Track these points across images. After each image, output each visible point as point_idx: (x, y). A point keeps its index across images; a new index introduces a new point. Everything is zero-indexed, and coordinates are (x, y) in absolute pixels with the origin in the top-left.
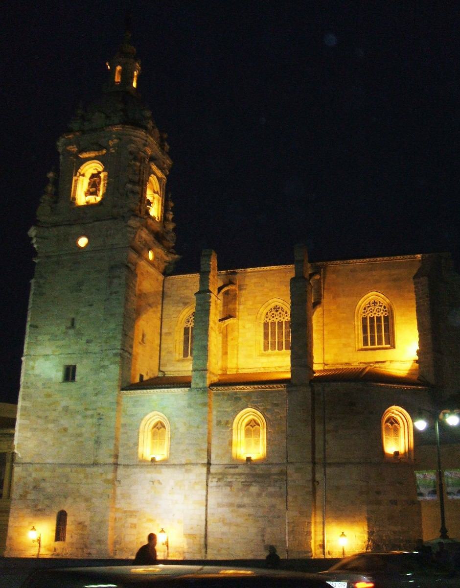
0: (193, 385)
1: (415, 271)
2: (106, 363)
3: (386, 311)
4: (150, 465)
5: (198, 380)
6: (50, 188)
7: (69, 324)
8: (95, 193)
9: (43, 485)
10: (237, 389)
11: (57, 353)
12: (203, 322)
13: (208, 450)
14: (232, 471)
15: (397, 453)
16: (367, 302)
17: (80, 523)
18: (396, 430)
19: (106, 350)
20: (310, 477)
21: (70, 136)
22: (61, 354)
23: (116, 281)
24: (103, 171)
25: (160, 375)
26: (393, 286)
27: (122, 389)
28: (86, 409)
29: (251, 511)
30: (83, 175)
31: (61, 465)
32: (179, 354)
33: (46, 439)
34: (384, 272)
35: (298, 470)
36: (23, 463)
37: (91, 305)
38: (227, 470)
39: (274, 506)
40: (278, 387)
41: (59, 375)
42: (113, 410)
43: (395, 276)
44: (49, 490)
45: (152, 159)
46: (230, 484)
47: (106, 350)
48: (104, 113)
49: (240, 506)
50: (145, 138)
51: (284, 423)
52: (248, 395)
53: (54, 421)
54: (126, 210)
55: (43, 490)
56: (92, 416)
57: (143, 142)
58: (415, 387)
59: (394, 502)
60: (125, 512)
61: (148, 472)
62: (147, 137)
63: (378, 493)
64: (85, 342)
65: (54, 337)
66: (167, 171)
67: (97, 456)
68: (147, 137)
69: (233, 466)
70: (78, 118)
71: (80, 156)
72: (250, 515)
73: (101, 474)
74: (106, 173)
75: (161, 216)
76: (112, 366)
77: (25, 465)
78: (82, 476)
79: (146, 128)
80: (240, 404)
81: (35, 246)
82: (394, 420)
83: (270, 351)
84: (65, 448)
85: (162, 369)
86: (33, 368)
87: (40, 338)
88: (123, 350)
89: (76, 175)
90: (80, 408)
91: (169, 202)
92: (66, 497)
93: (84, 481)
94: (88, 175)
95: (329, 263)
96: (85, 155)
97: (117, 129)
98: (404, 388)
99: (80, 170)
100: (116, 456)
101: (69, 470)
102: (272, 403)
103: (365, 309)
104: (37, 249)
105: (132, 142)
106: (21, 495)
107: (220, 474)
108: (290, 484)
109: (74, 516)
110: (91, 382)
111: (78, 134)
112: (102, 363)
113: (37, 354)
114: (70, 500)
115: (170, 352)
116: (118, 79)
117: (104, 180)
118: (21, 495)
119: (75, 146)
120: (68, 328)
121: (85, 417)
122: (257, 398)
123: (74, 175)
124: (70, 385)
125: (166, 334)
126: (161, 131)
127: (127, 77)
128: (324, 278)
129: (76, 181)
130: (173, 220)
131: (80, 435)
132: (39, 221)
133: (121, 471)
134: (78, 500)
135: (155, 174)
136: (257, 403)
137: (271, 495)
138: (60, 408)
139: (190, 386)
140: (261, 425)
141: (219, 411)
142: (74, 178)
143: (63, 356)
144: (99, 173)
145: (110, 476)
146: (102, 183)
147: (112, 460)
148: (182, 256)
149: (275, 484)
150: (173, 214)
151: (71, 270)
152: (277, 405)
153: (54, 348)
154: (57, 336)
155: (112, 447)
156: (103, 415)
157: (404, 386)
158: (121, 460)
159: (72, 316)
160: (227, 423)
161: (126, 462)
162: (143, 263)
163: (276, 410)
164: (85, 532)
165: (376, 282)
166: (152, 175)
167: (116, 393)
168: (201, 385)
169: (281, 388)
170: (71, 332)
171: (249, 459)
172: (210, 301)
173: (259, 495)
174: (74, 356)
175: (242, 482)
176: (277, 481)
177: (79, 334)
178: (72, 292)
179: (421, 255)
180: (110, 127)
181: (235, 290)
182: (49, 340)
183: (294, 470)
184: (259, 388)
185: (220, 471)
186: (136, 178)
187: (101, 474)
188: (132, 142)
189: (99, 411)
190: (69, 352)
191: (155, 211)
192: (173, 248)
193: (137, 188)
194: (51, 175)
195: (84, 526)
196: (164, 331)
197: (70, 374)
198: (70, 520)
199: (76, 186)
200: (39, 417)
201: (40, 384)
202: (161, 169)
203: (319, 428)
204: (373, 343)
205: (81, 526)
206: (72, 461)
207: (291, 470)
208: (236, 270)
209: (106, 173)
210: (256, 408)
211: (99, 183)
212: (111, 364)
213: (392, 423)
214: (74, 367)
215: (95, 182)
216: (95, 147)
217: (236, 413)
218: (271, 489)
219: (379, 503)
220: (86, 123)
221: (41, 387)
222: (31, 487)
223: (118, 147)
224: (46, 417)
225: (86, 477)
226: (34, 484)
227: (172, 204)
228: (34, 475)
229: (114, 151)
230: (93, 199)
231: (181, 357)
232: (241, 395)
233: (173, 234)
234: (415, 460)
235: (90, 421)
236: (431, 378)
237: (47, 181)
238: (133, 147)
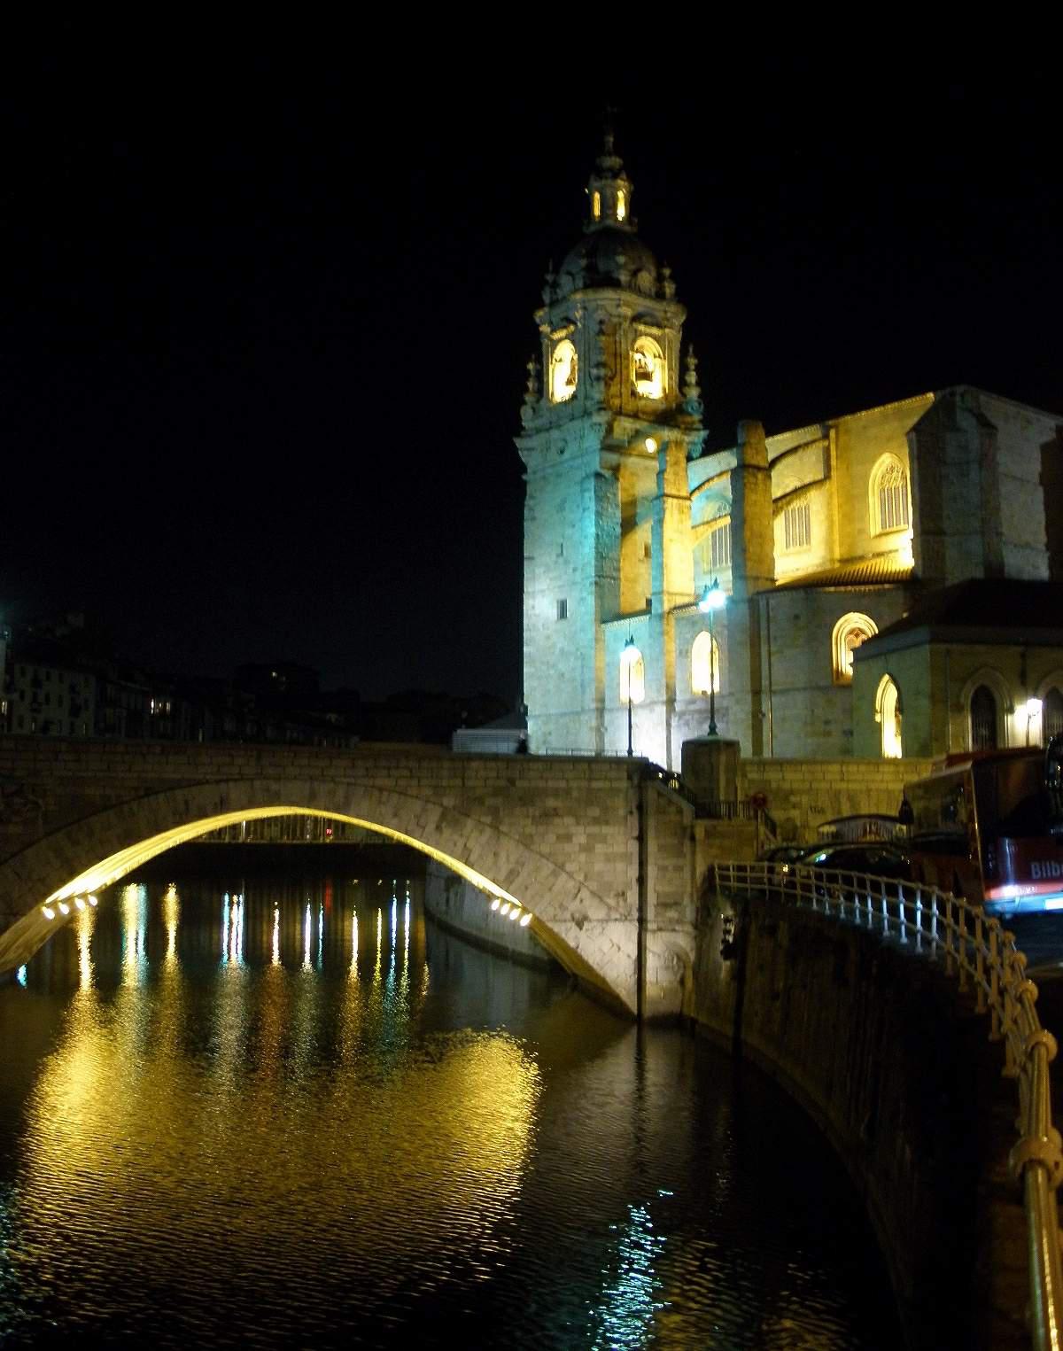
16: (883, 468)
27: (604, 622)
31: (564, 715)
35: (737, 702)
53: (554, 666)
57: (614, 303)
63: (827, 722)
80: (697, 629)
83: (792, 549)
86: (533, 607)
97: (579, 296)
120: (558, 556)
124: (563, 621)
127: (609, 205)
138: (557, 651)
147: (593, 706)
158: (608, 704)
159: (561, 540)
170: (561, 560)
177: (567, 562)
188: (597, 308)
200: (542, 663)
204: (720, 563)
217: (693, 638)
219: (828, 734)
237: (527, 374)
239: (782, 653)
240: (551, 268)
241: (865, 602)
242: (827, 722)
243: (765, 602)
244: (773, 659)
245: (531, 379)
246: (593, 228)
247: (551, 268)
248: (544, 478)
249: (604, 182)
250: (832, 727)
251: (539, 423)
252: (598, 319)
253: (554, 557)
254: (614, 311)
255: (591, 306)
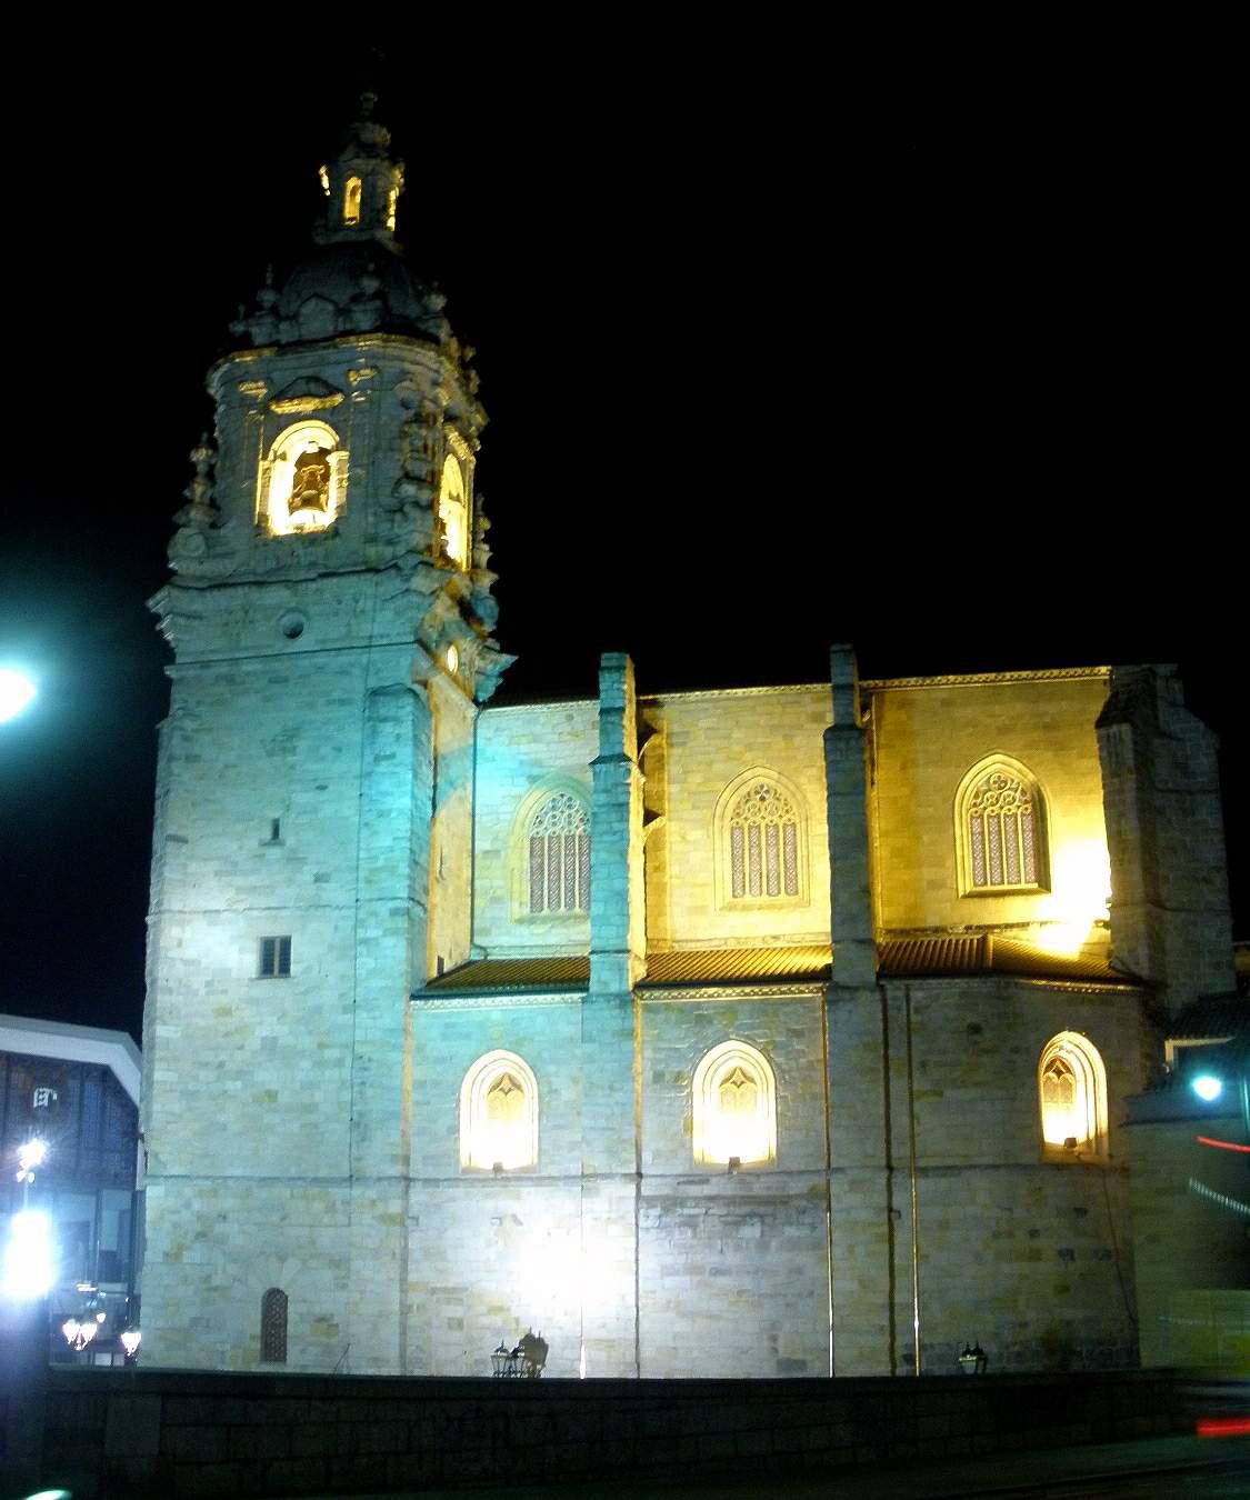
0: (594, 987)
1: (1096, 709)
2: (372, 933)
3: (1026, 802)
4: (493, 1180)
5: (606, 976)
6: (199, 489)
7: (267, 834)
8: (309, 502)
9: (220, 1228)
10: (701, 996)
11: (241, 906)
12: (615, 833)
13: (636, 1141)
14: (694, 1190)
15: (1071, 1142)
17: (321, 1319)
18: (1068, 1087)
19: (370, 900)
20: (882, 1201)
21: (248, 359)
22: (250, 909)
23: (388, 728)
24: (337, 448)
25: (476, 956)
26: (1045, 739)
27: (414, 997)
28: (322, 1046)
29: (748, 1283)
30: (283, 457)
32: (521, 904)
33: (221, 1118)
34: (1019, 707)
35: (854, 1186)
36: (166, 1177)
37: (322, 788)
38: (682, 1187)
39: (799, 1271)
40: (802, 992)
41: (251, 961)
42: (395, 1047)
43: (1047, 720)
44: (238, 1241)
45: (450, 418)
46: (690, 1223)
47: (370, 900)
48: (331, 301)
49: (717, 1272)
50: (435, 367)
51: (819, 1075)
52: (730, 1009)
53: (240, 1074)
54: (401, 550)
55: (222, 1241)
56: (339, 1063)
58: (1110, 987)
59: (1067, 1254)
60: (434, 1291)
61: (487, 1196)
62: (441, 363)
63: (1034, 1234)
64: (313, 878)
65: (230, 868)
66: (478, 442)
67: (358, 1159)
68: (441, 363)
69: (697, 1178)
70: (263, 312)
71: (273, 407)
72: (740, 1293)
73: (373, 1202)
74: (344, 455)
75: (468, 557)
76: (390, 941)
77: (171, 1180)
78: (318, 1206)
79: (435, 340)
80: (710, 1031)
81: (169, 636)
82: (1063, 1063)
83: (748, 898)
84: (271, 1139)
85: (478, 941)
86: (180, 944)
87: (193, 867)
88: (413, 899)
89: (265, 458)
90: (307, 1042)
91: (481, 520)
92: (282, 1259)
93: (326, 1220)
94: (293, 457)
95: (889, 683)
96: (287, 408)
98: (1087, 989)
99: (275, 446)
100: (406, 1160)
101: (287, 1192)
102: (789, 1030)
103: (976, 796)
104: (173, 645)
105: (404, 375)
106: (166, 1254)
107: (664, 1198)
108: (839, 1217)
109: (304, 1301)
110: (332, 980)
111: (267, 353)
112: (361, 933)
113: (186, 909)
114: (292, 1265)
115: (496, 900)
116: (351, 209)
117: (340, 471)
118: (166, 1254)
119: (261, 384)
121: (320, 1064)
122: (751, 1017)
123: (260, 457)
125: (487, 852)
126: (463, 345)
128: (880, 719)
129: (266, 470)
130: (492, 565)
131: (310, 1108)
132: (173, 573)
133: (418, 1195)
134: (313, 1263)
135: (455, 454)
136: (752, 1027)
137: (793, 1245)
139: (586, 989)
140: (758, 1081)
141: (657, 1050)
142: (262, 465)
143: (255, 913)
144: (324, 452)
145: (395, 1207)
146: (334, 477)
147: (397, 1170)
148: (516, 658)
149: (801, 1217)
150: (491, 550)
151: (267, 700)
152: (799, 1034)
153: (231, 894)
154: (235, 864)
155: (396, 1137)
156: (370, 1060)
157: (1088, 986)
159: (277, 815)
160: (679, 1076)
161: (431, 1173)
162: (439, 681)
163: (798, 1047)
164: (334, 1340)
165: (1004, 730)
166: (450, 456)
167: (401, 1005)
168: (614, 988)
169: (808, 992)
171: (734, 1163)
172: (628, 781)
173: (763, 1245)
174: (284, 913)
175: (721, 1216)
176: (804, 1212)
177: (295, 860)
178: (271, 754)
179: (1110, 668)
180: (352, 339)
181: (660, 746)
182: (217, 874)
183: (846, 1187)
184: (756, 994)
185: (666, 1191)
186: (422, 470)
187: (373, 1202)
188: (404, 375)
189: (360, 1049)
190: (272, 905)
191: (457, 543)
192: (491, 635)
193: (425, 496)
194: (200, 456)
195: (330, 1326)
196: (481, 845)
197: (275, 959)
198: (292, 1309)
199: (266, 486)
200: (205, 1065)
201: (198, 984)
202: (467, 438)
203: (899, 1086)
205: (324, 1325)
206: (293, 1172)
207: (838, 1186)
208: (661, 697)
209: (344, 455)
210: (750, 1040)
211: (326, 477)
212: (384, 935)
213: (1059, 1073)
214: (286, 943)
215: (312, 474)
216: (313, 387)
217: (701, 1053)
218: (791, 1231)
219: (1035, 1256)
220: (283, 326)
221: (202, 992)
222: (190, 1236)
223: (372, 389)
224: (221, 1065)
225: (331, 1209)
226: (198, 1227)
227: (485, 524)
228: (197, 1205)
229: (363, 399)
230: (318, 520)
231: (526, 911)
232: (711, 1011)
233: (491, 602)
234: (1110, 1156)
235: (332, 1074)
236: (1143, 970)
237: (190, 472)
238: (408, 388)
239: (941, 1094)
240: (269, 281)
241: (1085, 1010)
242: (1034, 1234)
243: (901, 994)
244: (917, 1106)
245: (199, 479)
246: (338, 238)
247: (269, 281)
248: (230, 680)
249: (373, 162)
250: (1042, 1243)
251: (212, 568)
252: (403, 395)
253: (252, 843)
254: (426, 387)
255: (391, 368)
